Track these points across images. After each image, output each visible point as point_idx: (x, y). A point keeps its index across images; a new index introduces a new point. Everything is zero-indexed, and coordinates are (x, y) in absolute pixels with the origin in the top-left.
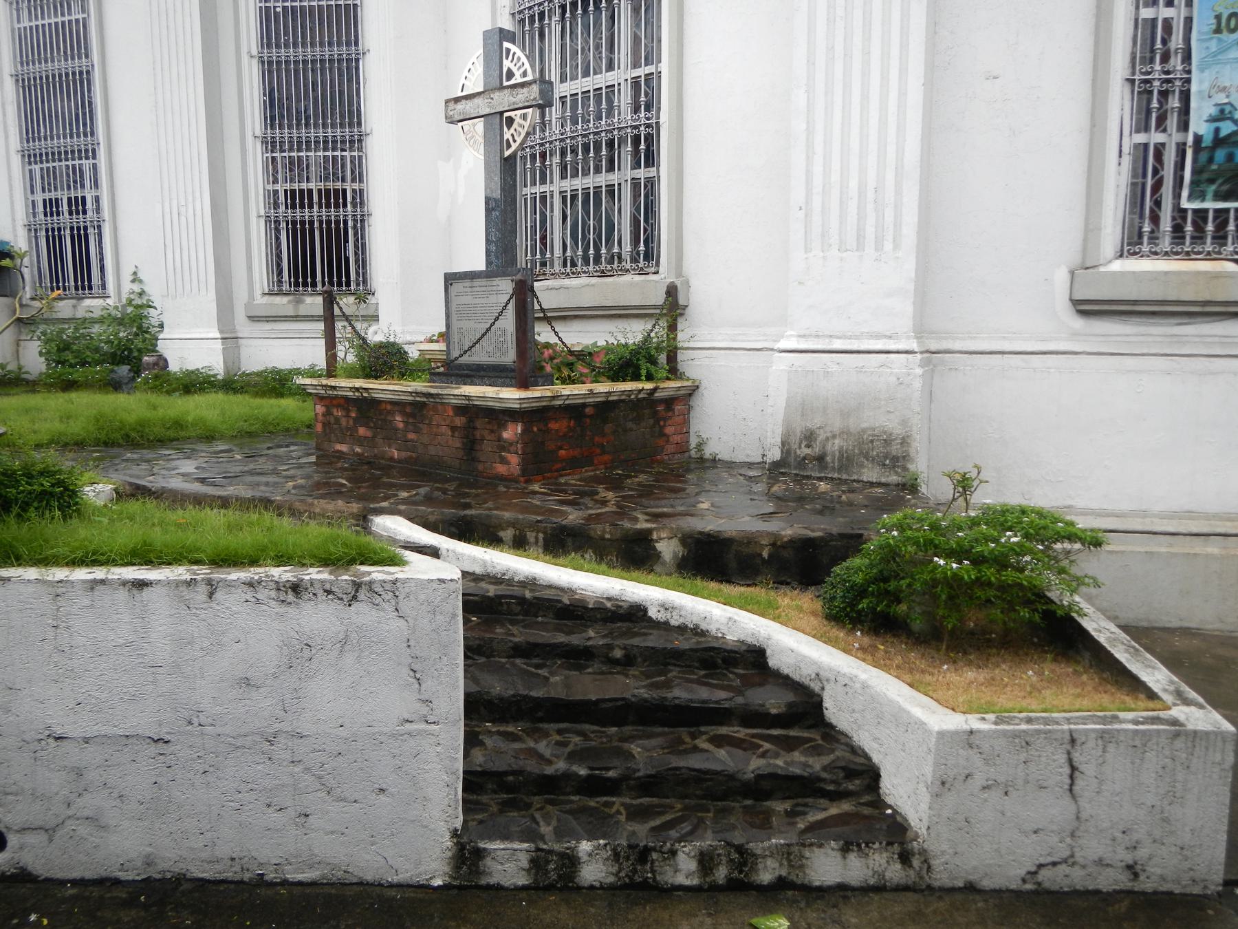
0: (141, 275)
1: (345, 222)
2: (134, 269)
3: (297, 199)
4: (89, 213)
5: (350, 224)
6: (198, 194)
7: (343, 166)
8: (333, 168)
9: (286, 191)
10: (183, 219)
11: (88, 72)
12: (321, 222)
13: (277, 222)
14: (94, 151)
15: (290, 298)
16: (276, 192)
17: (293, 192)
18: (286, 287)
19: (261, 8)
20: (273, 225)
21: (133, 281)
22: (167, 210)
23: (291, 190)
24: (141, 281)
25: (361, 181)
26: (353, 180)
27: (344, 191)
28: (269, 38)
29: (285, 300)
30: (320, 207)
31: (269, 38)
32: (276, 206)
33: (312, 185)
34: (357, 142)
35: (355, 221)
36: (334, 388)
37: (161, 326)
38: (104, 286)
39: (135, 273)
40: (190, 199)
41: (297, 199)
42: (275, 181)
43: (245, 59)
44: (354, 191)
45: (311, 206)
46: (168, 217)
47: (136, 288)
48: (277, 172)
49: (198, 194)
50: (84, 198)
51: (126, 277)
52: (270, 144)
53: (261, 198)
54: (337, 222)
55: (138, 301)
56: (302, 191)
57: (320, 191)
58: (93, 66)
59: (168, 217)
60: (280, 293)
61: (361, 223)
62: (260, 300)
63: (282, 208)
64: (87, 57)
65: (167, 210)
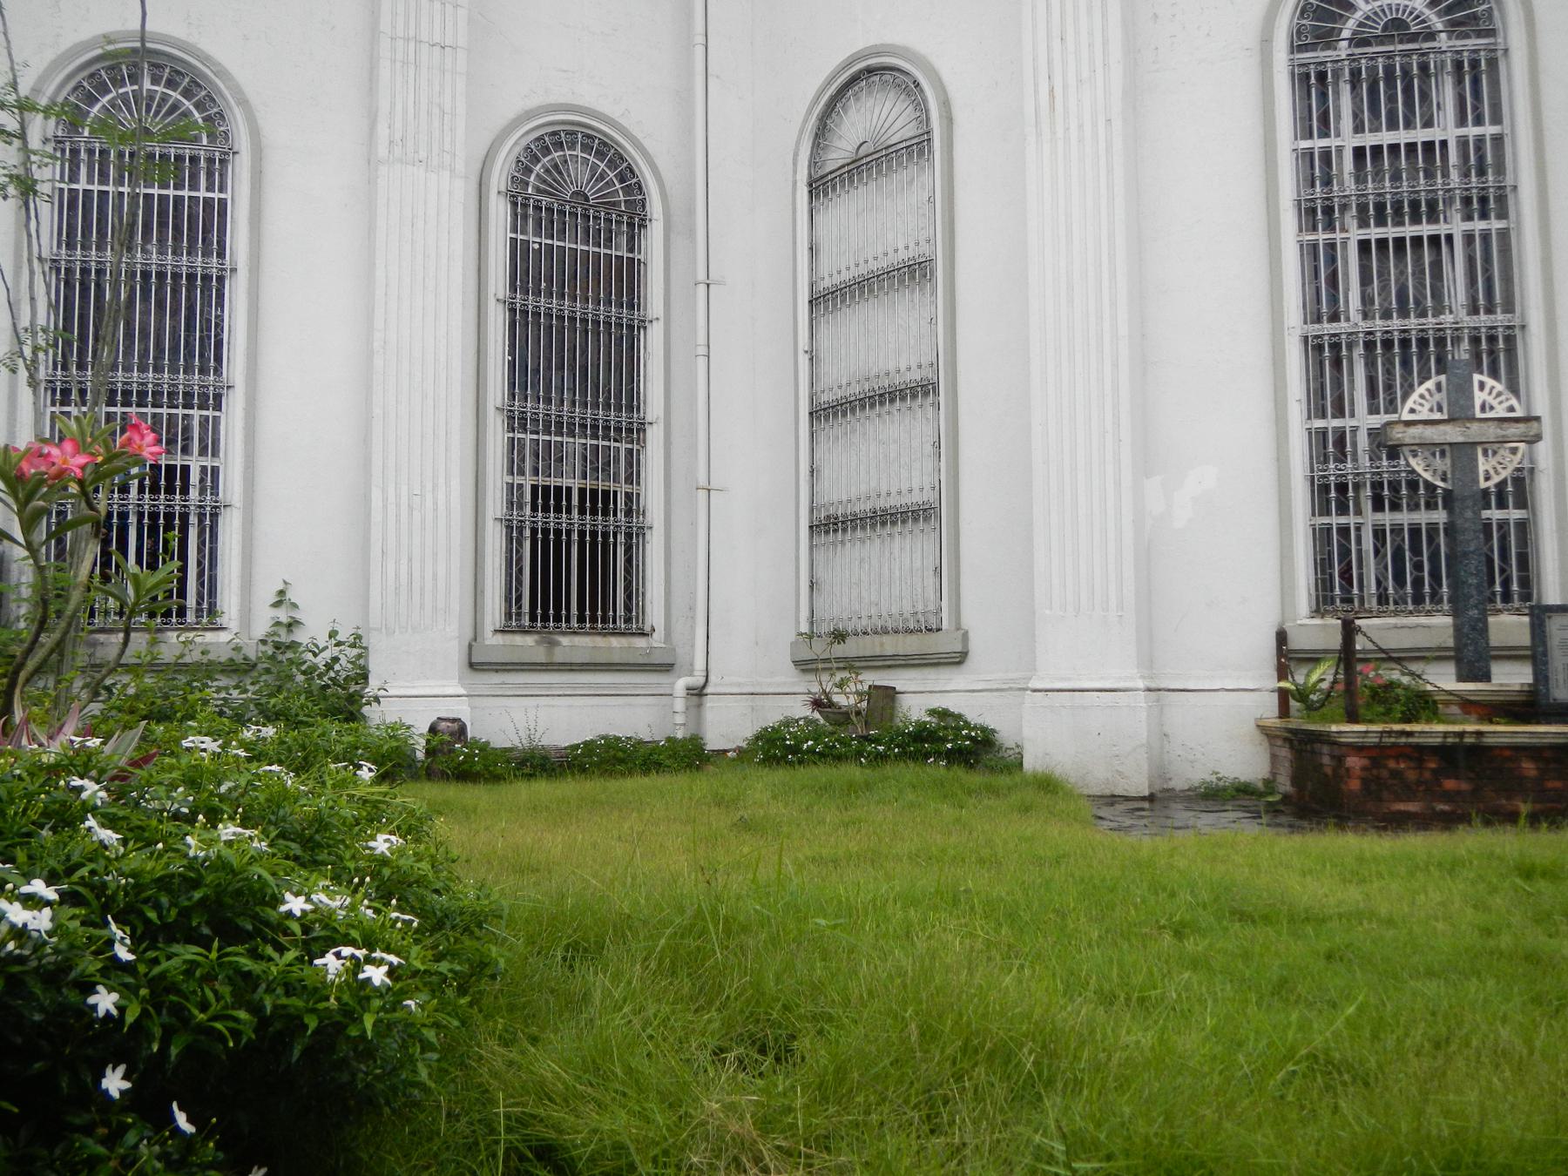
0: (291, 595)
1: (569, 533)
2: (281, 587)
3: (549, 499)
4: (194, 494)
5: (621, 538)
6: (442, 481)
7: (617, 460)
8: (596, 462)
9: (534, 488)
10: (416, 514)
11: (221, 279)
12: (582, 534)
13: (521, 530)
14: (218, 398)
15: (536, 637)
16: (520, 486)
17: (546, 489)
18: (526, 621)
19: (514, 241)
20: (512, 531)
21: (277, 605)
22: (392, 499)
23: (543, 487)
24: (295, 606)
25: (638, 484)
26: (629, 480)
27: (615, 493)
28: (525, 282)
29: (530, 640)
30: (582, 512)
31: (525, 282)
32: (521, 507)
33: (575, 484)
34: (636, 431)
35: (629, 536)
36: (1410, 734)
37: (364, 677)
38: (212, 611)
39: (282, 593)
40: (429, 486)
41: (549, 499)
42: (522, 472)
43: (492, 303)
44: (629, 496)
45: (569, 511)
46: (392, 509)
47: (283, 615)
48: (523, 460)
49: (442, 481)
50: (186, 470)
51: (265, 593)
52: (516, 421)
53: (499, 494)
54: (558, 532)
55: (284, 637)
56: (558, 489)
57: (582, 491)
58: (234, 270)
59: (392, 509)
60: (523, 631)
61: (634, 538)
62: (491, 639)
63: (528, 510)
64: (221, 255)
65: (392, 499)
